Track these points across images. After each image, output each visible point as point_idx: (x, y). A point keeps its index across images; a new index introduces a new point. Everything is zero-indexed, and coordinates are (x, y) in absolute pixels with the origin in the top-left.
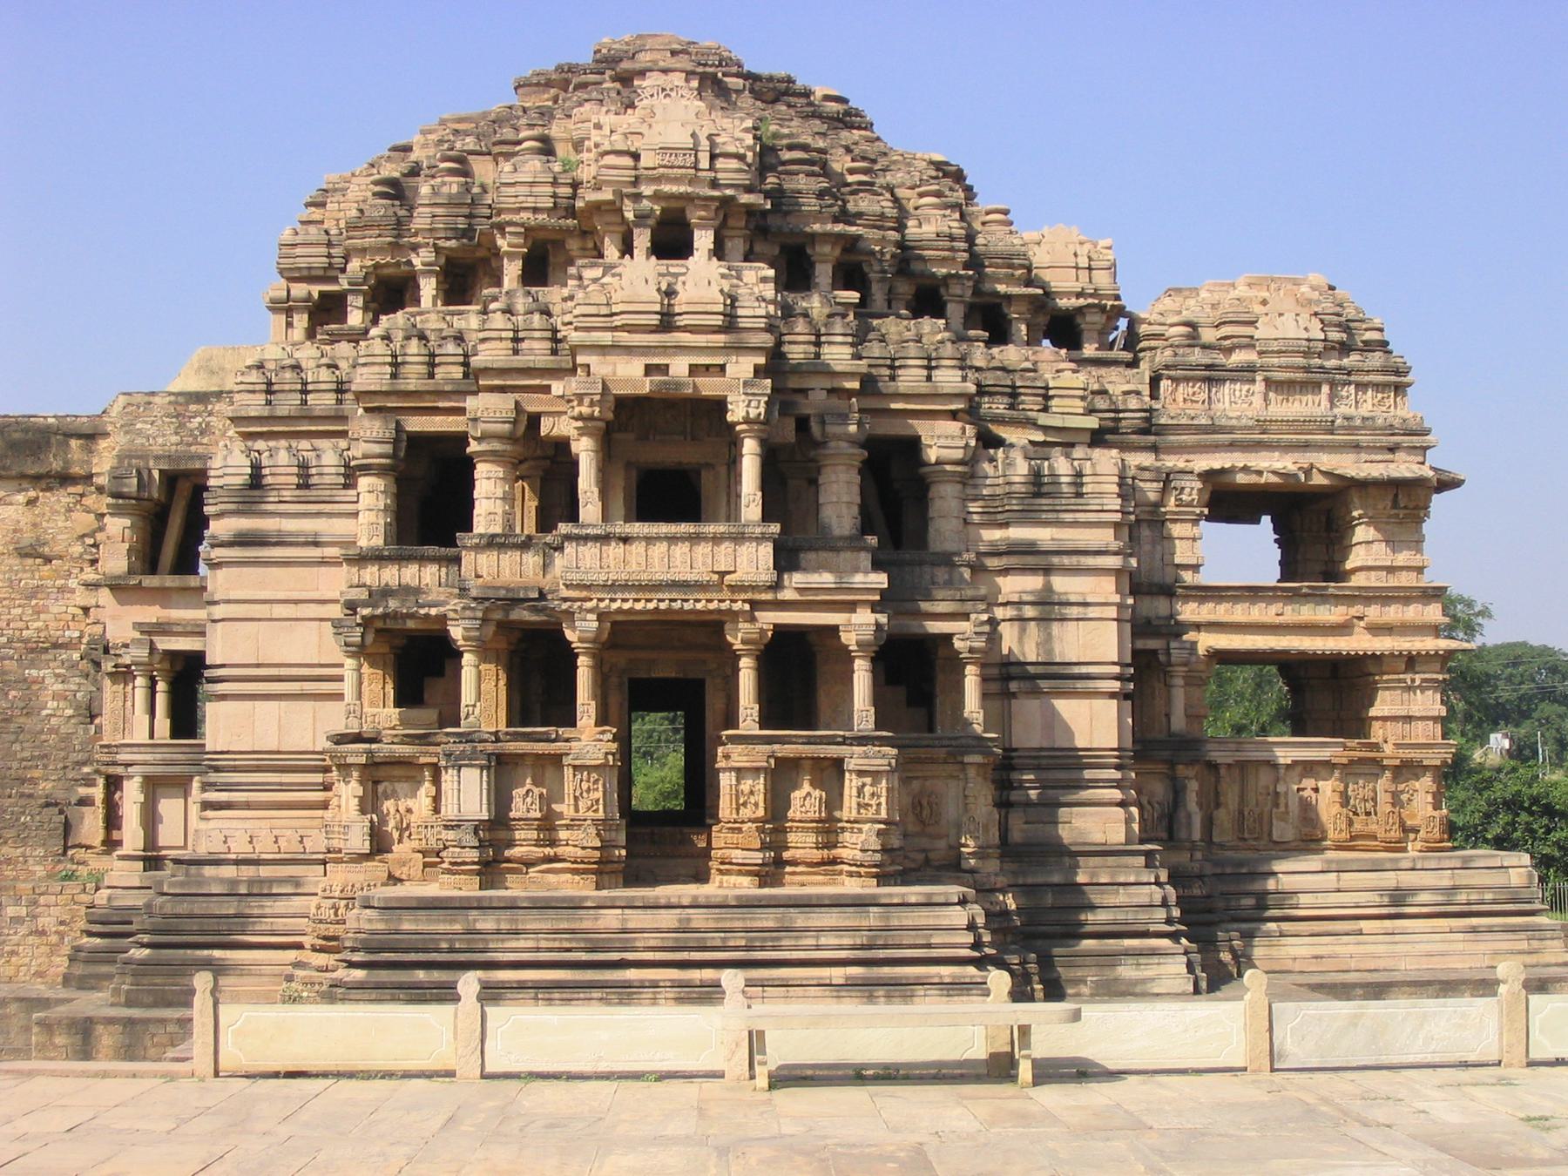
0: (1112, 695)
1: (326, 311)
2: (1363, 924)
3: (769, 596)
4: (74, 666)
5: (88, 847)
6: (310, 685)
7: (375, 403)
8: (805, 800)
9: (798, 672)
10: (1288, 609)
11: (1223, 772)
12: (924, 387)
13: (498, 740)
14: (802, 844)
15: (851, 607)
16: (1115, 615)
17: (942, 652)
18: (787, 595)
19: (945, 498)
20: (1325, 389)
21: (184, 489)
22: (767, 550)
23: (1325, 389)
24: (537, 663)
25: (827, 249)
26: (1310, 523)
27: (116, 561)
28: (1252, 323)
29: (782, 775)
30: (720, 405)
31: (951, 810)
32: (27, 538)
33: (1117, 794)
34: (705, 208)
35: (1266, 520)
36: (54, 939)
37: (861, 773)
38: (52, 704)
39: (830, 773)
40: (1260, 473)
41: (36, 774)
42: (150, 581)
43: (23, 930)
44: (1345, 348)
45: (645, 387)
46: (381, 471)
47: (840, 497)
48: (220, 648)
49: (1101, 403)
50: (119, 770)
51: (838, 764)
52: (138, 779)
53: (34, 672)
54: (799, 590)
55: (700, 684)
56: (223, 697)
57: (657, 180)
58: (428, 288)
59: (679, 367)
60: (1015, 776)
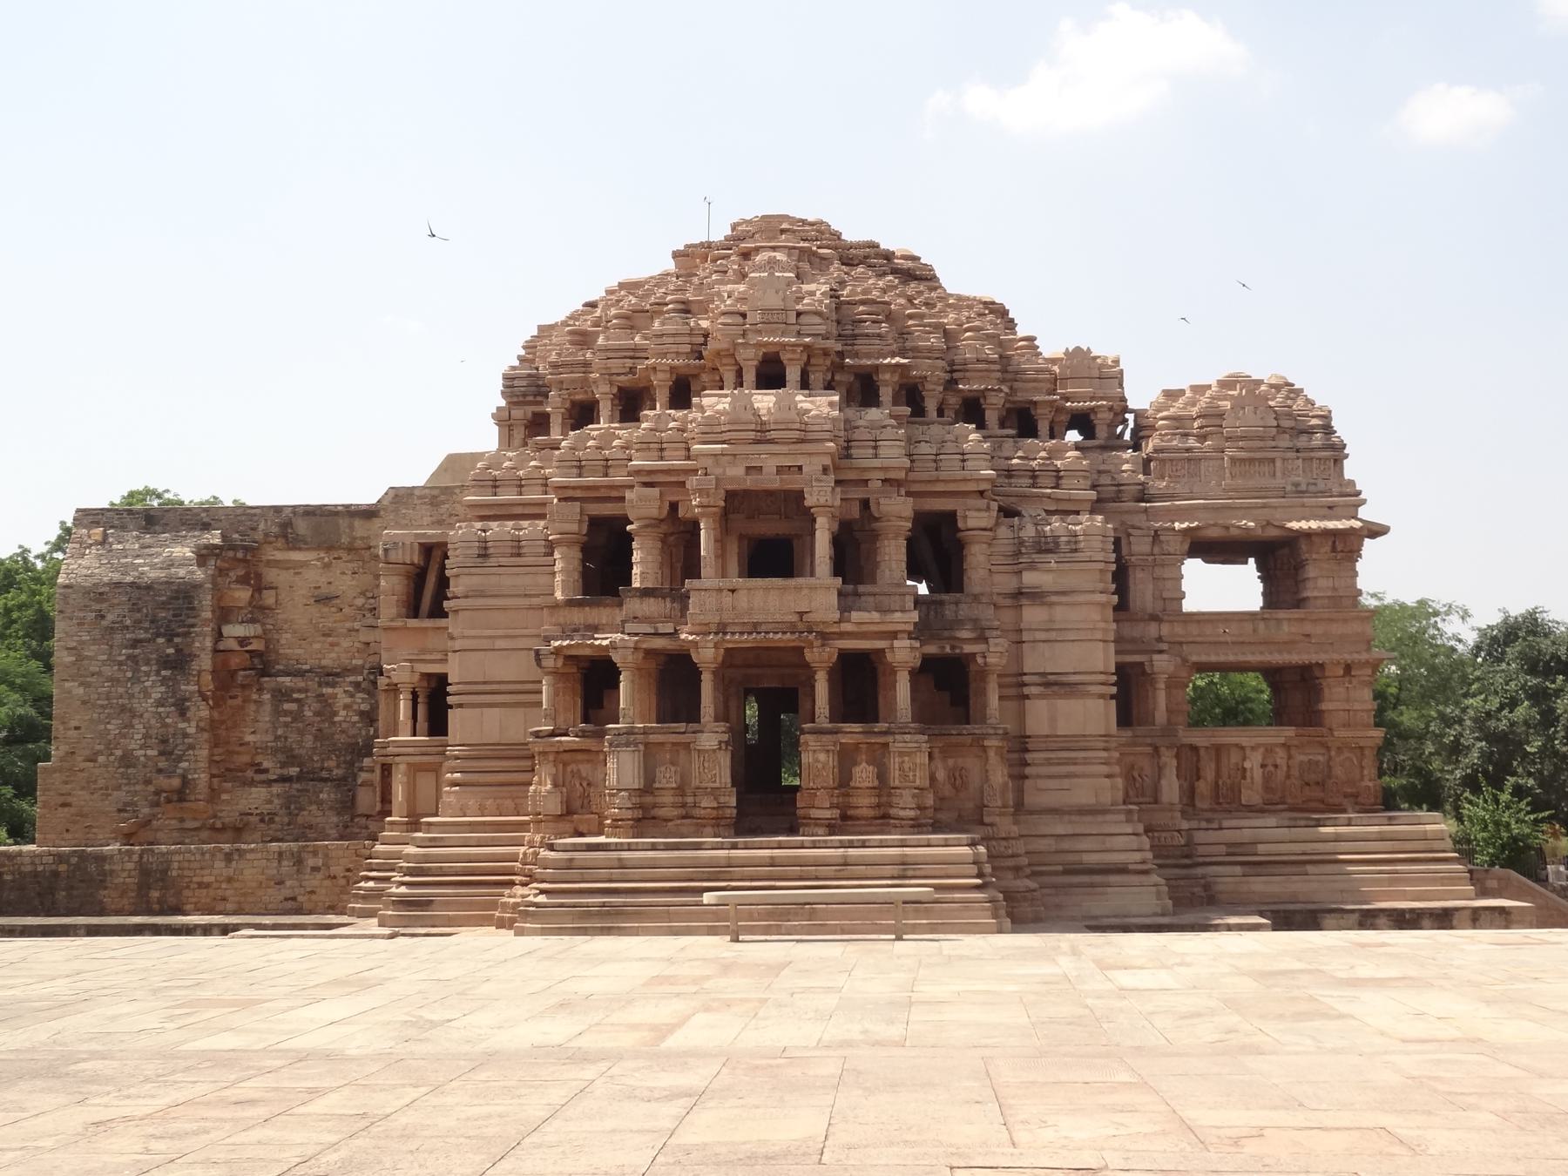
0: (1102, 696)
1: (539, 424)
2: (1309, 868)
4: (357, 685)
5: (368, 816)
6: (522, 695)
7: (567, 495)
8: (864, 774)
9: (859, 681)
11: (1202, 752)
12: (960, 474)
14: (864, 803)
15: (894, 635)
17: (973, 668)
21: (437, 554)
22: (833, 599)
24: (675, 680)
25: (887, 376)
26: (1280, 560)
27: (389, 608)
29: (846, 758)
30: (800, 495)
31: (975, 779)
32: (325, 590)
33: (1105, 769)
34: (794, 352)
35: (1252, 561)
36: (342, 882)
38: (343, 713)
39: (879, 754)
40: (1227, 528)
41: (331, 763)
42: (413, 623)
43: (319, 876)
45: (750, 483)
46: (570, 544)
47: (893, 555)
48: (455, 671)
49: (1105, 480)
50: (389, 760)
51: (886, 745)
52: (402, 767)
53: (330, 690)
55: (795, 691)
56: (460, 706)
57: (759, 332)
58: (605, 409)
59: (770, 465)
60: (1028, 756)
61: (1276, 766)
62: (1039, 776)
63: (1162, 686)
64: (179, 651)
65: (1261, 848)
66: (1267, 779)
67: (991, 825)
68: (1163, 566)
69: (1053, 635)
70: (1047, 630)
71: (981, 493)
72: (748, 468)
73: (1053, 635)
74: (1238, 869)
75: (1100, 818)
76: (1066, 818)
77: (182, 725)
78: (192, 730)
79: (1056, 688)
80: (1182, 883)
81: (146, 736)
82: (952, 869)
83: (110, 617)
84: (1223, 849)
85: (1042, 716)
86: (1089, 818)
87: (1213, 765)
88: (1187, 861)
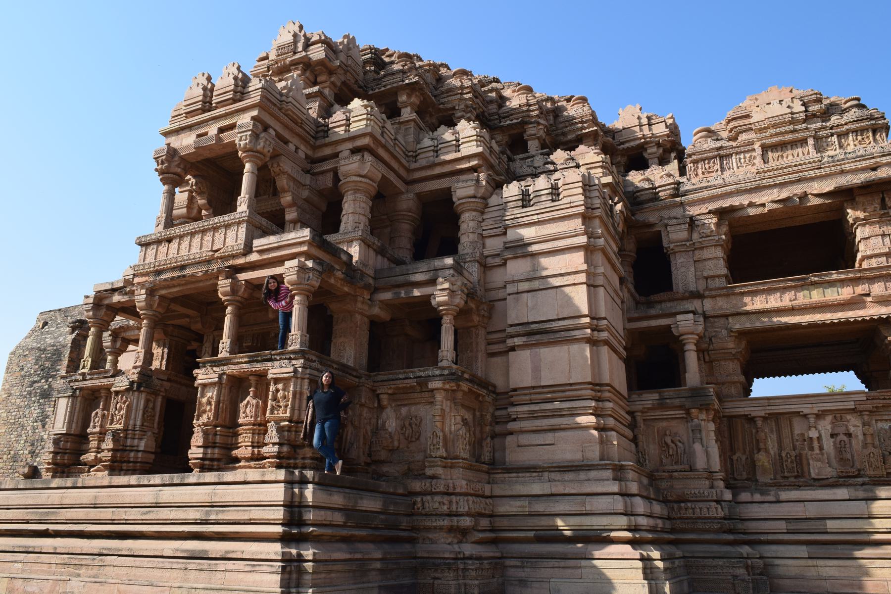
3: (241, 261)
10: (800, 295)
13: (84, 380)
16: (584, 280)
18: (254, 257)
19: (468, 222)
20: (811, 141)
23: (811, 141)
28: (748, 116)
37: (277, 381)
40: (763, 205)
44: (826, 114)
54: (260, 252)
61: (849, 435)
62: (522, 432)
63: (692, 347)
64: (50, 386)
65: (831, 525)
66: (840, 449)
67: (433, 477)
68: (702, 248)
69: (536, 284)
70: (530, 280)
71: (474, 169)
72: (199, 136)
73: (536, 284)
74: (803, 551)
75: (582, 475)
76: (546, 474)
77: (42, 434)
78: (45, 437)
79: (538, 337)
80: (721, 562)
81: (26, 441)
82: (256, 514)
83: (26, 369)
84: (782, 525)
85: (525, 368)
86: (570, 476)
87: (774, 437)
88: (731, 537)
